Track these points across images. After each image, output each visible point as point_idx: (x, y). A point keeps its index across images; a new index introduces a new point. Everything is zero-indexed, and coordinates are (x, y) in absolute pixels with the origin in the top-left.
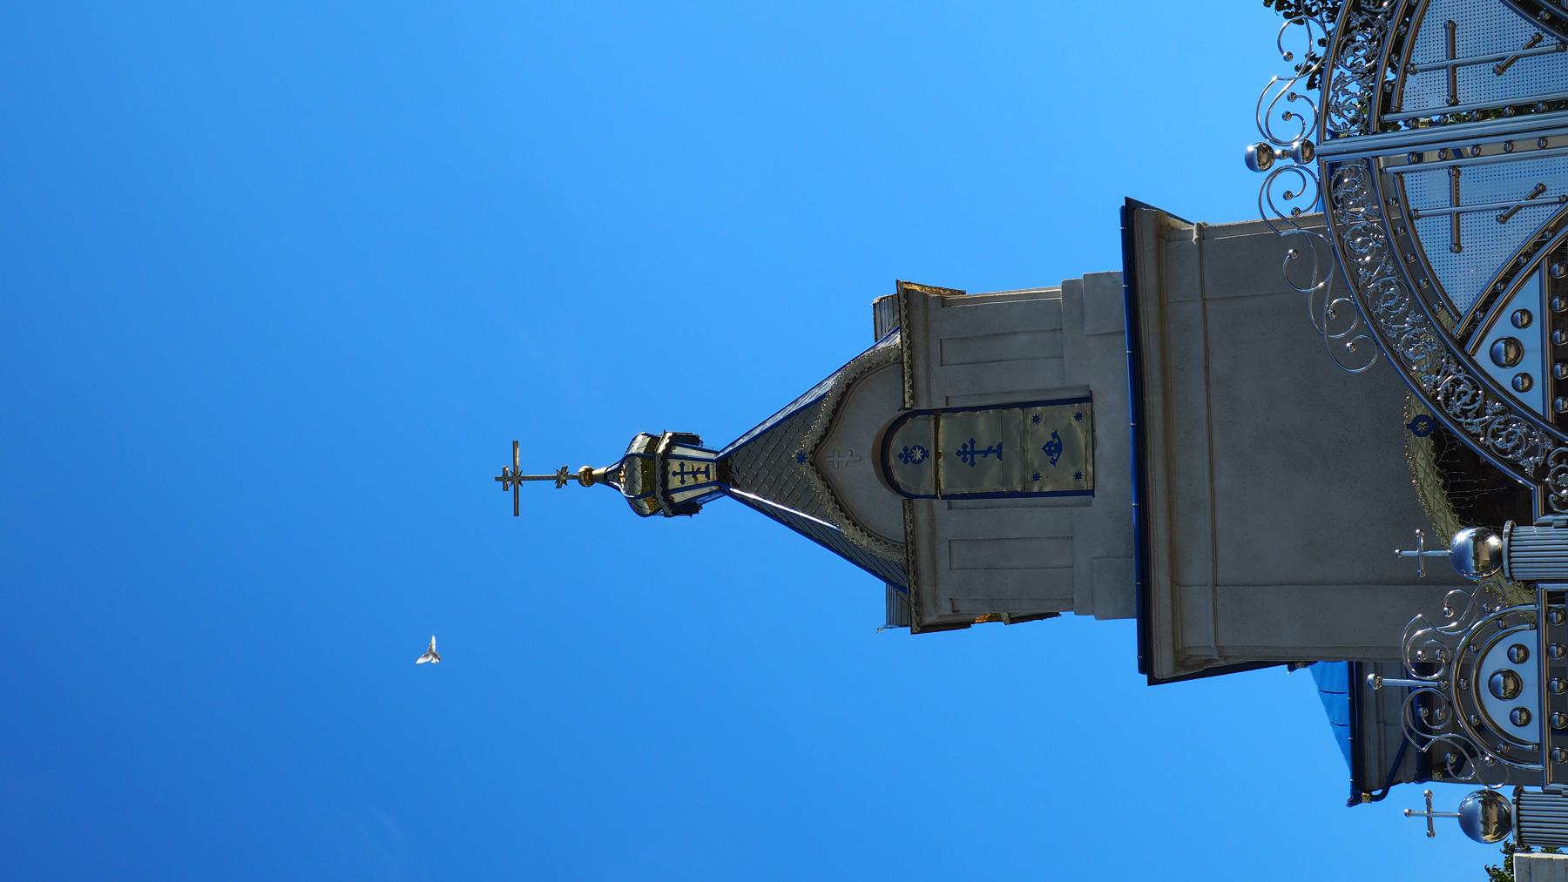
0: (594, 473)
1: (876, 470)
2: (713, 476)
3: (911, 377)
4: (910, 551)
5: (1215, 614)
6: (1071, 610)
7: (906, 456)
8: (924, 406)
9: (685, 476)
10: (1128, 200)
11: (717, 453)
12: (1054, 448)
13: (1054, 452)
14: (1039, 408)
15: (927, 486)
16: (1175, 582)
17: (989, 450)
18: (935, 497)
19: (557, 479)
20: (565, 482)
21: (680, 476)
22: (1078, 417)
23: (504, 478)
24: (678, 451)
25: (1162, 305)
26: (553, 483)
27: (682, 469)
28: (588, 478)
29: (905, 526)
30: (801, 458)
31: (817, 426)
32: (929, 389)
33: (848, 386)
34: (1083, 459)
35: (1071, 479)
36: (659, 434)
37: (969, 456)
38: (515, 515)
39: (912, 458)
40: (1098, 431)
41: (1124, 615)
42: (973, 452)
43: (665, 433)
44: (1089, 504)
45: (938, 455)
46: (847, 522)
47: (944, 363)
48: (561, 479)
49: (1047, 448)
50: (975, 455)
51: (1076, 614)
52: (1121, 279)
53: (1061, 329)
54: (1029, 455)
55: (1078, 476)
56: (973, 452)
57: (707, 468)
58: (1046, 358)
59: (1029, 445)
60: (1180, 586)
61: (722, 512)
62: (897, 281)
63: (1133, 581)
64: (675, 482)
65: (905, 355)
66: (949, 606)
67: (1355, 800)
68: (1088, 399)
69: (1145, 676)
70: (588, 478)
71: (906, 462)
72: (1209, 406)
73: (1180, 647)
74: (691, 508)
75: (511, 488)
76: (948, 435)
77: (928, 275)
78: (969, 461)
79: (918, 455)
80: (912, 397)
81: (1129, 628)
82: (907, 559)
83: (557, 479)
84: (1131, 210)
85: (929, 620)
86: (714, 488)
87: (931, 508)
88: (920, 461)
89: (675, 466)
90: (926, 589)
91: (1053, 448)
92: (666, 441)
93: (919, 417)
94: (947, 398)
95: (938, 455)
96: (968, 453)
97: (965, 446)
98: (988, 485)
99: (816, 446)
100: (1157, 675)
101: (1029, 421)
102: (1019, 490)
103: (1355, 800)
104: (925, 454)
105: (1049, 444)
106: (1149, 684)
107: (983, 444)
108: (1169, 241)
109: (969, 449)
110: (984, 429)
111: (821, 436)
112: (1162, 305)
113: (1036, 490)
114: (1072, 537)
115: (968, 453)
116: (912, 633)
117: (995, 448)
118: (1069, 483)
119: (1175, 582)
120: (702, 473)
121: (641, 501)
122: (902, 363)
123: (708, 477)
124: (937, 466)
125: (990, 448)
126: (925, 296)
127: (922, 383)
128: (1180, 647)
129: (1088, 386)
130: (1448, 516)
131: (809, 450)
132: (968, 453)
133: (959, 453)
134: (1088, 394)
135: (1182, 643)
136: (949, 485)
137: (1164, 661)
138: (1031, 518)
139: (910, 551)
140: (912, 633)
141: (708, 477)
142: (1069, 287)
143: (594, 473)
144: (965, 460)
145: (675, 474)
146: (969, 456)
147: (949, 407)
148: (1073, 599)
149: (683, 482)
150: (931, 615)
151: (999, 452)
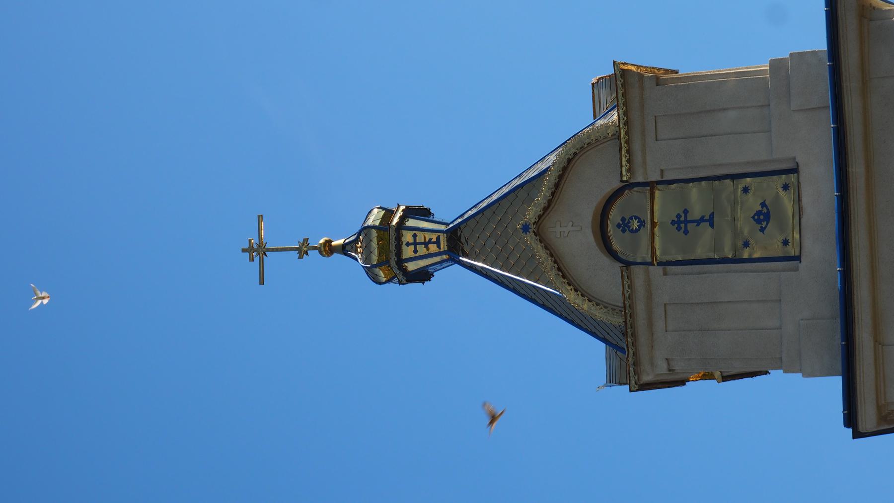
0: (333, 244)
1: (595, 240)
2: (444, 246)
3: (628, 152)
4: (628, 315)
6: (780, 368)
7: (624, 226)
8: (640, 179)
9: (418, 246)
11: (447, 224)
12: (763, 217)
14: (748, 180)
15: (643, 254)
16: (878, 342)
17: (703, 219)
18: (652, 264)
19: (299, 250)
20: (306, 253)
22: (785, 187)
23: (250, 250)
24: (411, 223)
26: (295, 254)
27: (415, 240)
28: (328, 249)
29: (623, 291)
30: (526, 228)
31: (541, 199)
32: (644, 163)
33: (569, 161)
35: (779, 245)
36: (394, 208)
37: (682, 225)
38: (260, 284)
39: (629, 227)
40: (805, 200)
42: (686, 222)
43: (399, 206)
44: (796, 269)
45: (653, 224)
46: (569, 288)
47: (659, 137)
48: (303, 250)
49: (756, 217)
50: (689, 225)
51: (785, 372)
52: (826, 57)
53: (769, 105)
54: (740, 224)
55: (786, 243)
56: (686, 222)
57: (438, 238)
59: (740, 215)
60: (883, 346)
62: (614, 62)
63: (838, 341)
64: (408, 252)
65: (622, 131)
66: (665, 366)
68: (795, 170)
69: (850, 431)
70: (328, 249)
71: (624, 231)
74: (423, 276)
75: (257, 259)
78: (683, 229)
79: (635, 224)
80: (629, 171)
81: (836, 383)
82: (625, 322)
83: (299, 250)
85: (646, 378)
86: (445, 257)
88: (637, 231)
89: (408, 237)
90: (643, 350)
91: (762, 217)
92: (400, 214)
93: (635, 189)
94: (662, 171)
95: (653, 224)
96: (682, 222)
97: (678, 216)
98: (701, 252)
99: (540, 217)
100: (862, 428)
102: (730, 257)
104: (642, 223)
105: (759, 213)
106: (854, 437)
107: (696, 214)
108: (871, 20)
109: (682, 219)
111: (544, 207)
113: (746, 256)
114: (780, 300)
115: (682, 222)
116: (631, 391)
117: (707, 218)
118: (777, 249)
119: (878, 342)
120: (434, 243)
121: (377, 270)
122: (619, 138)
123: (439, 246)
124: (653, 235)
125: (703, 217)
126: (640, 76)
127: (638, 158)
128: (883, 402)
129: (794, 158)
131: (533, 221)
132: (682, 222)
133: (673, 222)
137: (868, 416)
139: (628, 315)
140: (631, 391)
141: (439, 246)
142: (776, 65)
143: (333, 244)
144: (679, 229)
145: (408, 244)
146: (682, 225)
147: (665, 178)
148: (781, 359)
149: (415, 251)
151: (711, 221)
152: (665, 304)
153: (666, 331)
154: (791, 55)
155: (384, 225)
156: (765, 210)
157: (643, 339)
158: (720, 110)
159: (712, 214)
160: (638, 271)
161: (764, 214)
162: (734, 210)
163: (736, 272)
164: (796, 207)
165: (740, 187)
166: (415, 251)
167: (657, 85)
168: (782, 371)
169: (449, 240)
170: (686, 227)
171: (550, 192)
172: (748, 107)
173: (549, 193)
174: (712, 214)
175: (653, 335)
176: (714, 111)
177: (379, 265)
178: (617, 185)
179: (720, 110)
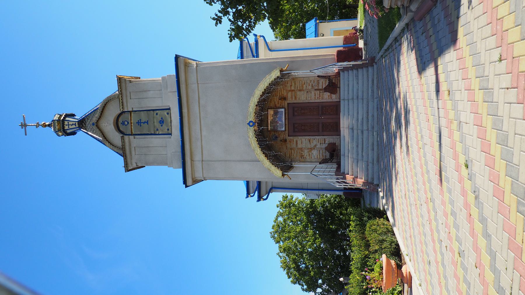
3: (122, 102)
5: (202, 168)
8: (126, 110)
10: (176, 55)
12: (162, 122)
13: (162, 123)
14: (157, 111)
17: (145, 122)
21: (69, 126)
25: (187, 85)
29: (122, 143)
31: (97, 115)
32: (127, 106)
33: (105, 105)
35: (166, 130)
37: (140, 124)
41: (181, 168)
42: (141, 123)
44: (170, 138)
45: (131, 123)
46: (107, 142)
47: (131, 98)
50: (141, 124)
51: (168, 167)
53: (162, 90)
54: (155, 124)
55: (168, 130)
56: (141, 123)
57: (75, 123)
58: (158, 98)
61: (81, 134)
62: (117, 75)
66: (135, 164)
67: (247, 197)
68: (169, 109)
71: (123, 125)
72: (200, 112)
73: (194, 177)
76: (134, 118)
77: (126, 74)
79: (126, 123)
81: (181, 170)
84: (177, 57)
85: (130, 168)
87: (129, 138)
88: (127, 125)
91: (161, 122)
94: (132, 108)
96: (140, 123)
97: (138, 121)
99: (97, 121)
101: (155, 114)
102: (153, 133)
103: (247, 197)
104: (128, 123)
105: (161, 121)
107: (143, 121)
108: (188, 67)
109: (139, 122)
110: (144, 117)
112: (187, 85)
113: (157, 133)
115: (139, 123)
116: (127, 170)
117: (146, 122)
118: (166, 131)
119: (192, 160)
126: (125, 80)
127: (125, 104)
128: (194, 177)
129: (169, 106)
130: (258, 149)
132: (140, 123)
133: (137, 123)
134: (169, 108)
135: (194, 176)
138: (155, 141)
140: (127, 170)
142: (163, 78)
144: (139, 125)
146: (140, 124)
148: (167, 163)
150: (130, 167)
152: (135, 147)
153: (135, 155)
154: (167, 75)
156: (162, 120)
158: (148, 91)
160: (126, 137)
161: (162, 121)
162: (154, 120)
163: (154, 138)
167: (130, 83)
168: (167, 166)
169: (78, 124)
170: (140, 124)
171: (100, 113)
172: (156, 90)
173: (100, 114)
175: (131, 156)
176: (147, 91)
178: (120, 112)
179: (148, 91)
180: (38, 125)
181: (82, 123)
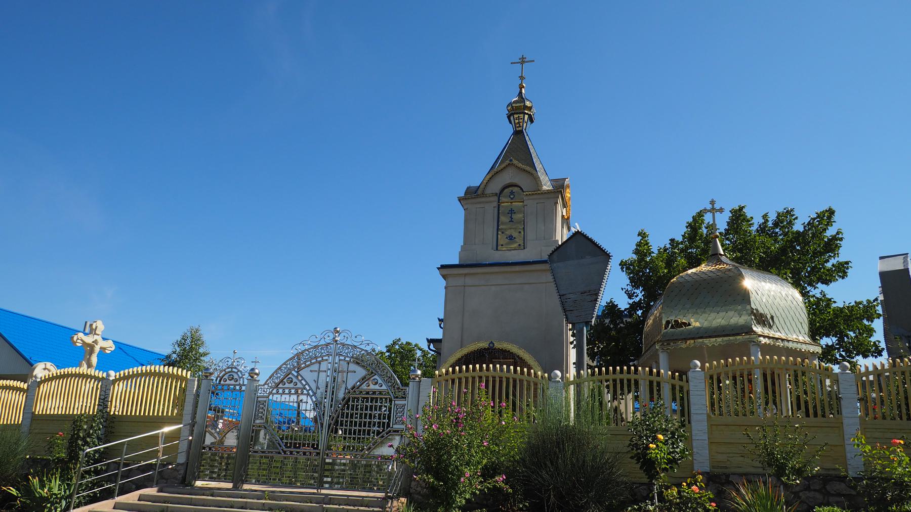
7: (512, 193)
11: (525, 130)
12: (511, 238)
15: (502, 199)
18: (499, 202)
19: (522, 76)
22: (520, 245)
23: (523, 58)
28: (521, 87)
34: (507, 246)
36: (532, 110)
40: (513, 251)
54: (509, 231)
55: (502, 245)
56: (512, 213)
59: (512, 230)
64: (516, 116)
70: (521, 87)
83: (522, 76)
89: (522, 116)
90: (470, 201)
95: (511, 203)
97: (514, 211)
98: (502, 218)
101: (519, 230)
104: (512, 199)
105: (512, 236)
107: (514, 216)
113: (499, 233)
115: (512, 212)
118: (500, 242)
121: (510, 106)
123: (518, 127)
124: (508, 202)
136: (503, 206)
143: (523, 89)
144: (510, 211)
151: (511, 221)
155: (526, 107)
157: (473, 200)
159: (513, 221)
162: (513, 228)
164: (513, 249)
165: (521, 231)
166: (516, 119)
174: (513, 221)
177: (512, 107)
180: (522, 78)
181: (519, 134)
